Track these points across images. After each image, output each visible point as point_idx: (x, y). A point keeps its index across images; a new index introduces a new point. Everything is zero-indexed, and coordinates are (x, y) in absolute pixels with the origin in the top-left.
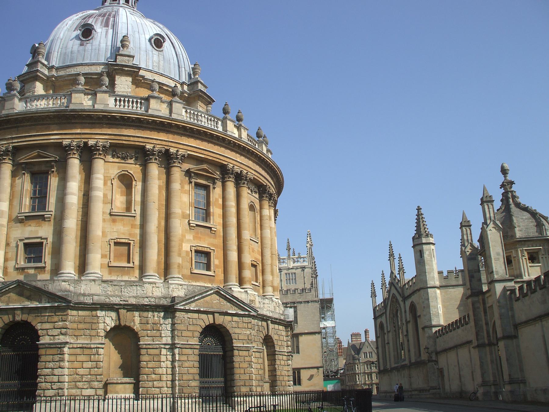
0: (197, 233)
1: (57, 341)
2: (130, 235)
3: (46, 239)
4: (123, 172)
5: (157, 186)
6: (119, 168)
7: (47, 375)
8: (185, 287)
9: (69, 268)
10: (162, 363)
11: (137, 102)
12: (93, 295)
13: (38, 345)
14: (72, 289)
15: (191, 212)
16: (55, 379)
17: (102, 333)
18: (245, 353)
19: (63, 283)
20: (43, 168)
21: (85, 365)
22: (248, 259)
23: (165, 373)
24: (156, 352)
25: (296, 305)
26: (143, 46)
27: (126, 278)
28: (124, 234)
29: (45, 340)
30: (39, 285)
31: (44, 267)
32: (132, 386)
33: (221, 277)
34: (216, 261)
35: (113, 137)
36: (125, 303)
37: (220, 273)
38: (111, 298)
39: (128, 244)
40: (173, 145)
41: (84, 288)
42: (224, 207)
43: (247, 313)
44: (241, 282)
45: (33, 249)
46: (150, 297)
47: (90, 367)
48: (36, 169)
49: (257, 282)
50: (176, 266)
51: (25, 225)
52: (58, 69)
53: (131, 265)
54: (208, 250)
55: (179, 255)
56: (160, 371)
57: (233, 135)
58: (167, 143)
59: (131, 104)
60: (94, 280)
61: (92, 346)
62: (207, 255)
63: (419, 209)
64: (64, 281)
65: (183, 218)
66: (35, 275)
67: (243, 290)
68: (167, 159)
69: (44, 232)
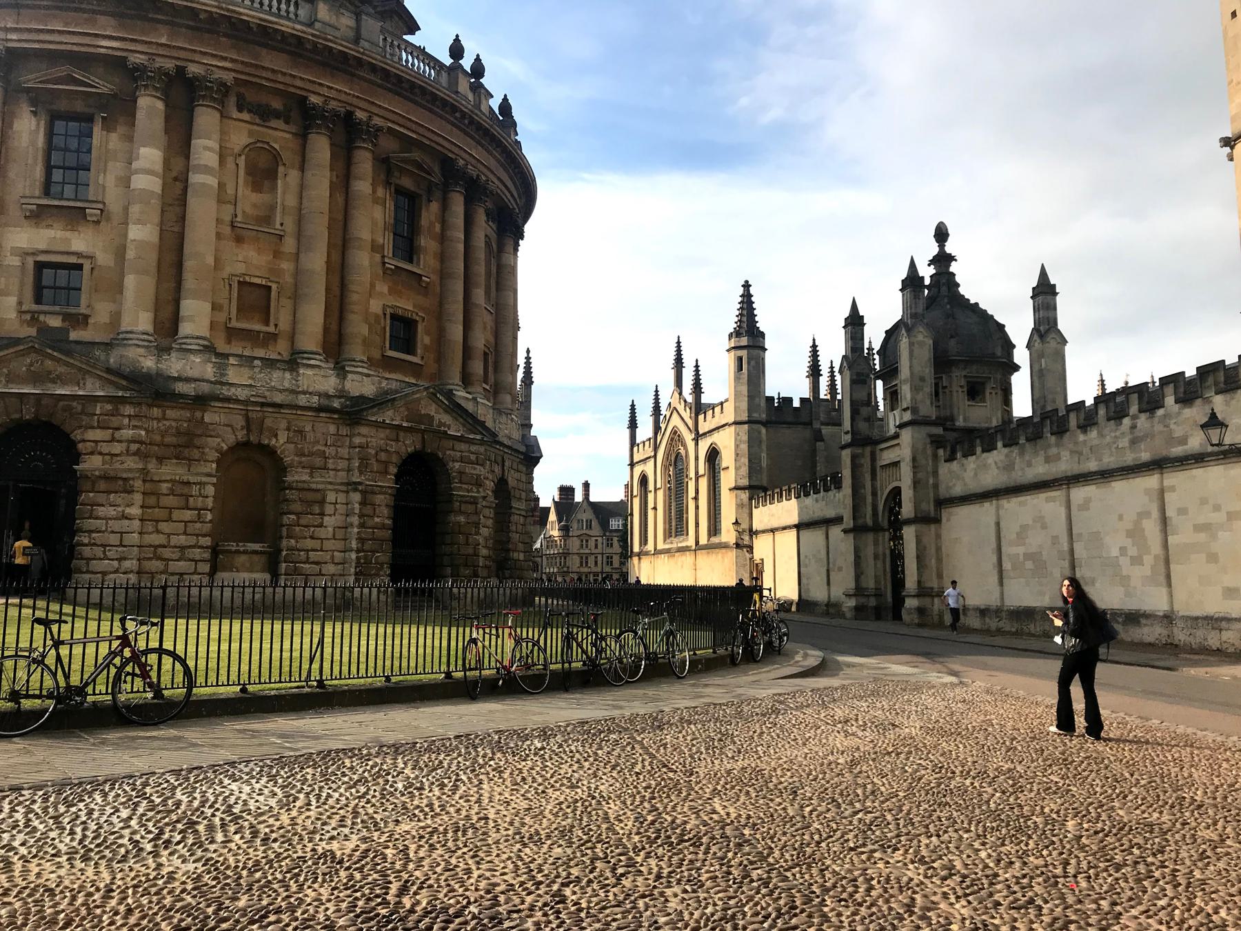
1: (117, 465)
3: (87, 257)
4: (259, 145)
6: (251, 133)
7: (92, 531)
10: (326, 518)
13: (75, 471)
14: (149, 363)
15: (387, 241)
16: (114, 539)
17: (214, 455)
18: (470, 508)
20: (79, 107)
21: (176, 515)
23: (330, 536)
24: (318, 496)
27: (260, 353)
29: (91, 464)
31: (86, 317)
32: (263, 559)
35: (239, 67)
39: (270, 287)
41: (174, 365)
42: (443, 239)
43: (478, 437)
44: (466, 380)
47: (189, 518)
48: (62, 105)
51: (37, 225)
53: (271, 329)
54: (415, 317)
56: (321, 533)
61: (192, 479)
63: (747, 286)
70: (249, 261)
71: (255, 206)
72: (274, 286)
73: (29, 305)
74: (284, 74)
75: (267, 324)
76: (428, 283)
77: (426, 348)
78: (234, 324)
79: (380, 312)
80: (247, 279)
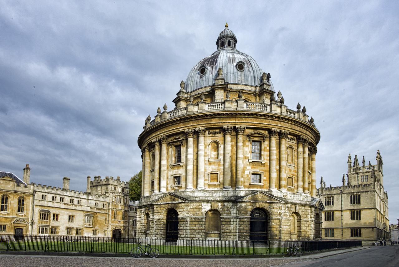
0: (253, 165)
2: (218, 169)
5: (230, 146)
8: (244, 191)
9: (190, 186)
11: (219, 105)
12: (200, 197)
14: (191, 194)
15: (250, 156)
19: (188, 193)
22: (284, 175)
25: (360, 193)
26: (232, 71)
28: (215, 169)
30: (178, 194)
31: (181, 186)
33: (268, 185)
34: (264, 178)
36: (214, 200)
37: (267, 184)
38: (208, 198)
39: (218, 173)
40: (238, 124)
41: (196, 194)
44: (280, 187)
45: (177, 179)
46: (226, 197)
49: (292, 186)
50: (240, 182)
52: (191, 93)
54: (260, 173)
55: (242, 177)
57: (276, 112)
58: (235, 124)
59: (216, 107)
60: (200, 191)
62: (260, 175)
64: (188, 192)
65: (246, 159)
66: (178, 190)
67: (279, 191)
68: (236, 130)
69: (181, 171)
70: (213, 168)
71: (214, 155)
72: (219, 173)
73: (173, 185)
74: (217, 123)
75: (218, 182)
76: (264, 164)
77: (264, 180)
78: (210, 183)
79: (249, 174)
80: (213, 172)
